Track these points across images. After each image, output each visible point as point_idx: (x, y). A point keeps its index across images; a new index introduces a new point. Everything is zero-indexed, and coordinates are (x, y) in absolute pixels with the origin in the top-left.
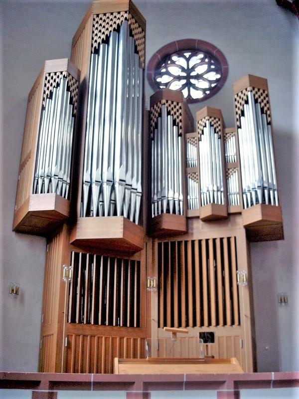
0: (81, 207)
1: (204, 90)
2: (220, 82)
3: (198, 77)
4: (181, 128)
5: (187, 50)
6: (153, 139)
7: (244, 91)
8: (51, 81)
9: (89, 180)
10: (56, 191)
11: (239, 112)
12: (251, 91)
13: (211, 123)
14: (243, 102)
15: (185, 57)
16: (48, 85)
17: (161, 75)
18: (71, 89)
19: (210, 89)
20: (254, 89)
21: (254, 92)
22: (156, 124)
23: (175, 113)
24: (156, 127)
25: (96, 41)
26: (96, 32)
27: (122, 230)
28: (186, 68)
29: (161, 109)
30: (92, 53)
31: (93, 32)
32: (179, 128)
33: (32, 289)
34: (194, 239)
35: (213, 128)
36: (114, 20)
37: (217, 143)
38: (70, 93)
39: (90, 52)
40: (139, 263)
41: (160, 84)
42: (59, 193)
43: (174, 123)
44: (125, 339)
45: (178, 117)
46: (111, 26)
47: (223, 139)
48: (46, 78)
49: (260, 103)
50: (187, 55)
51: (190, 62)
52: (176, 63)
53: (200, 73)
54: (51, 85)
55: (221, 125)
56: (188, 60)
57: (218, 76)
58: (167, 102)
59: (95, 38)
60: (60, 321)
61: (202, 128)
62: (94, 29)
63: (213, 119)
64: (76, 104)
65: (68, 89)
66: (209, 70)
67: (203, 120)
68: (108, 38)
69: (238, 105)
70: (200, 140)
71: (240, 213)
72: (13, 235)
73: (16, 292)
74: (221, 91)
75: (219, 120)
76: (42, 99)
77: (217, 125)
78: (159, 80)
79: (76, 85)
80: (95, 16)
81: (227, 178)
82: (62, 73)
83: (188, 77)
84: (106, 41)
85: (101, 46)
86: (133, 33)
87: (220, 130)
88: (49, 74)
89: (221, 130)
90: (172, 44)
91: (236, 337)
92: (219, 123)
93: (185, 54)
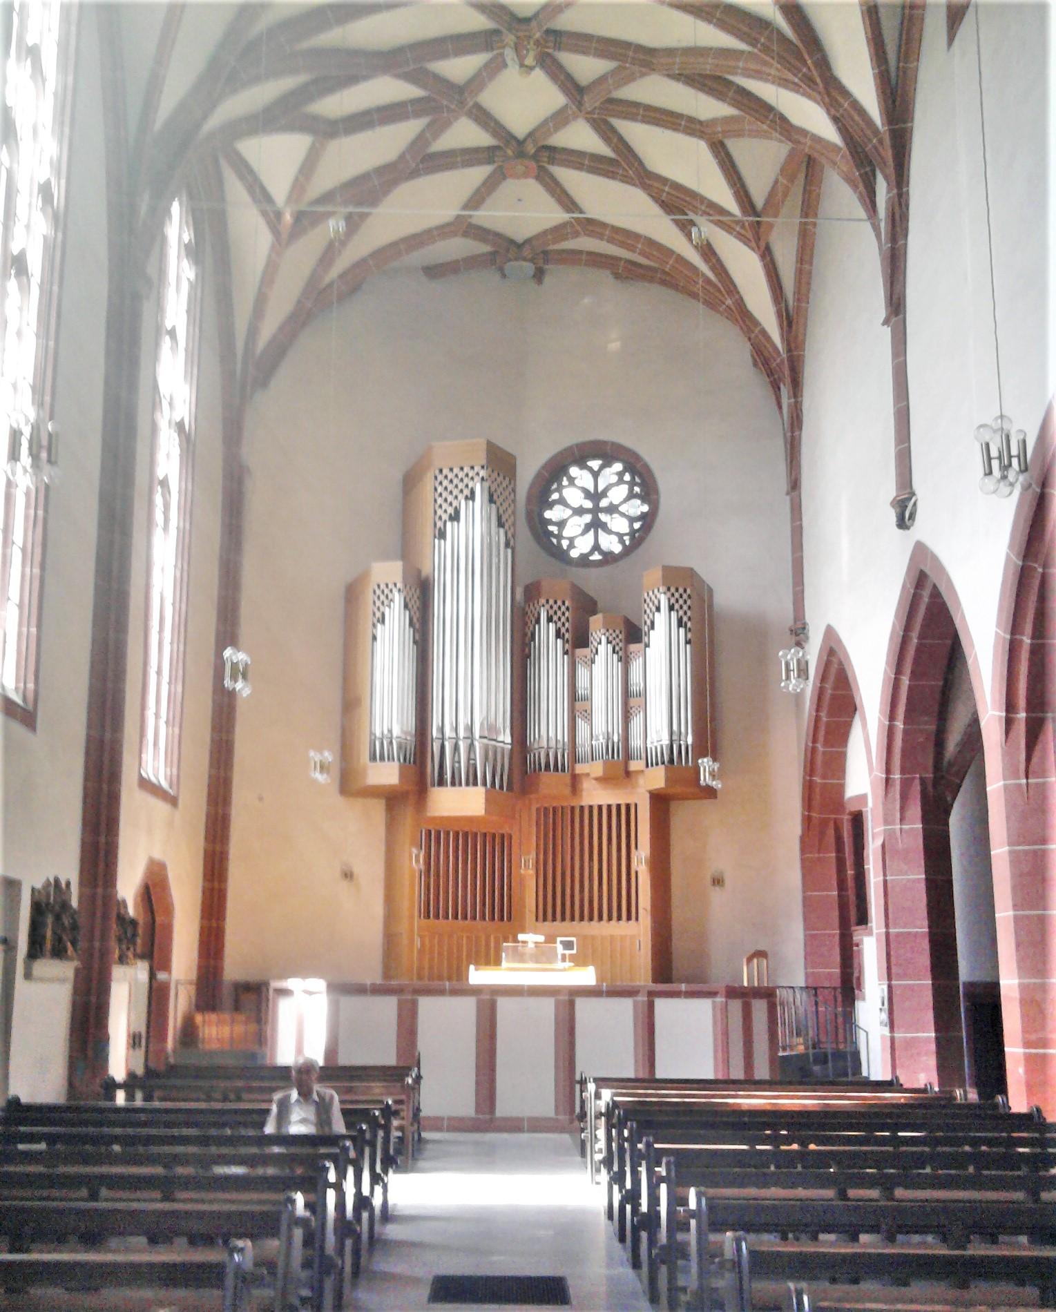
0: (432, 769)
1: (620, 536)
2: (648, 520)
3: (612, 509)
4: (568, 641)
5: (595, 457)
6: (529, 656)
7: (656, 591)
8: (382, 597)
9: (440, 736)
10: (399, 760)
11: (649, 622)
12: (665, 593)
13: (608, 638)
14: (654, 609)
15: (590, 469)
16: (378, 603)
17: (550, 506)
18: (410, 606)
19: (633, 533)
20: (669, 589)
21: (669, 594)
22: (533, 635)
23: (559, 619)
24: (533, 638)
25: (440, 518)
26: (440, 489)
27: (483, 806)
28: (592, 491)
29: (539, 614)
30: (435, 537)
31: (435, 501)
32: (566, 641)
33: (371, 870)
34: (583, 804)
35: (610, 647)
36: (466, 480)
37: (618, 667)
38: (407, 613)
39: (432, 537)
40: (510, 837)
41: (550, 522)
42: (402, 760)
43: (558, 634)
44: (492, 937)
45: (563, 624)
46: (461, 491)
47: (625, 661)
48: (374, 592)
49: (677, 611)
50: (595, 464)
51: (600, 480)
52: (576, 482)
53: (616, 502)
54: (383, 603)
55: (623, 640)
56: (596, 475)
57: (645, 508)
58: (547, 601)
59: (440, 512)
60: (412, 917)
61: (596, 645)
62: (437, 485)
63: (611, 631)
64: (417, 626)
65: (406, 606)
66: (631, 496)
67: (598, 632)
68: (457, 511)
69: (648, 611)
70: (593, 662)
71: (642, 771)
72: (339, 801)
73: (348, 875)
74: (644, 545)
75: (621, 633)
76: (371, 623)
77: (617, 640)
78: (548, 514)
79: (415, 597)
80: (437, 472)
81: (629, 714)
82: (395, 585)
83: (596, 511)
84: (455, 517)
85: (449, 524)
86: (495, 497)
87: (621, 649)
88: (379, 586)
89: (623, 648)
90: (569, 450)
91: (632, 937)
92: (620, 637)
93: (590, 463)
